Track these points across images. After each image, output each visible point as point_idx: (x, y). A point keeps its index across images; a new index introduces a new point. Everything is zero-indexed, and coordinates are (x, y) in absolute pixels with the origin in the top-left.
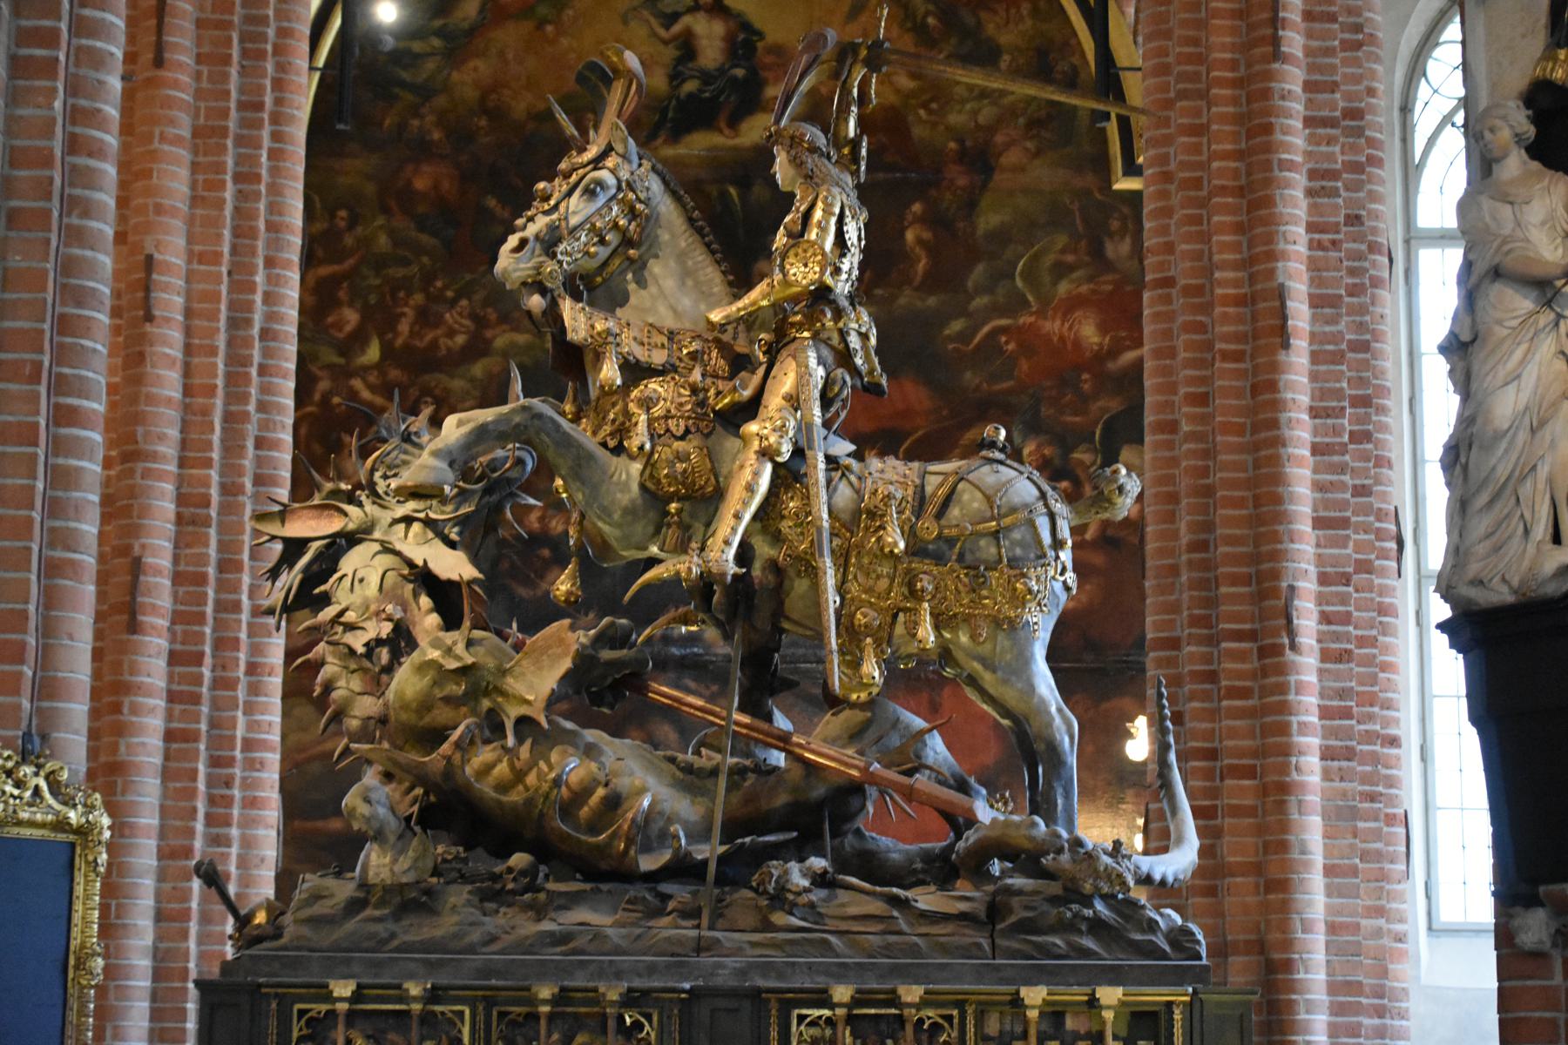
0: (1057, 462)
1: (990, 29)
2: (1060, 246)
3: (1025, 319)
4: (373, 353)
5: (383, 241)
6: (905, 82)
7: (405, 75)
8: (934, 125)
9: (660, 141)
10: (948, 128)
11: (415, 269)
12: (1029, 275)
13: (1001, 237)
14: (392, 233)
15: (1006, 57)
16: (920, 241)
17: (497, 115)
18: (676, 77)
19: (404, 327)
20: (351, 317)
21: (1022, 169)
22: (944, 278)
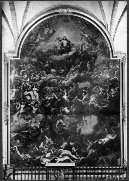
0: (104, 91)
1: (97, 41)
2: (104, 66)
3: (101, 75)
4: (28, 80)
5: (29, 67)
6: (87, 48)
7: (31, 48)
8: (90, 52)
9: (60, 55)
10: (92, 53)
11: (33, 70)
12: (101, 70)
13: (98, 65)
14: (30, 66)
15: (99, 44)
16: (89, 66)
17: (41, 52)
18: (61, 48)
19: (32, 77)
20: (26, 76)
21: (100, 57)
22: (92, 70)
